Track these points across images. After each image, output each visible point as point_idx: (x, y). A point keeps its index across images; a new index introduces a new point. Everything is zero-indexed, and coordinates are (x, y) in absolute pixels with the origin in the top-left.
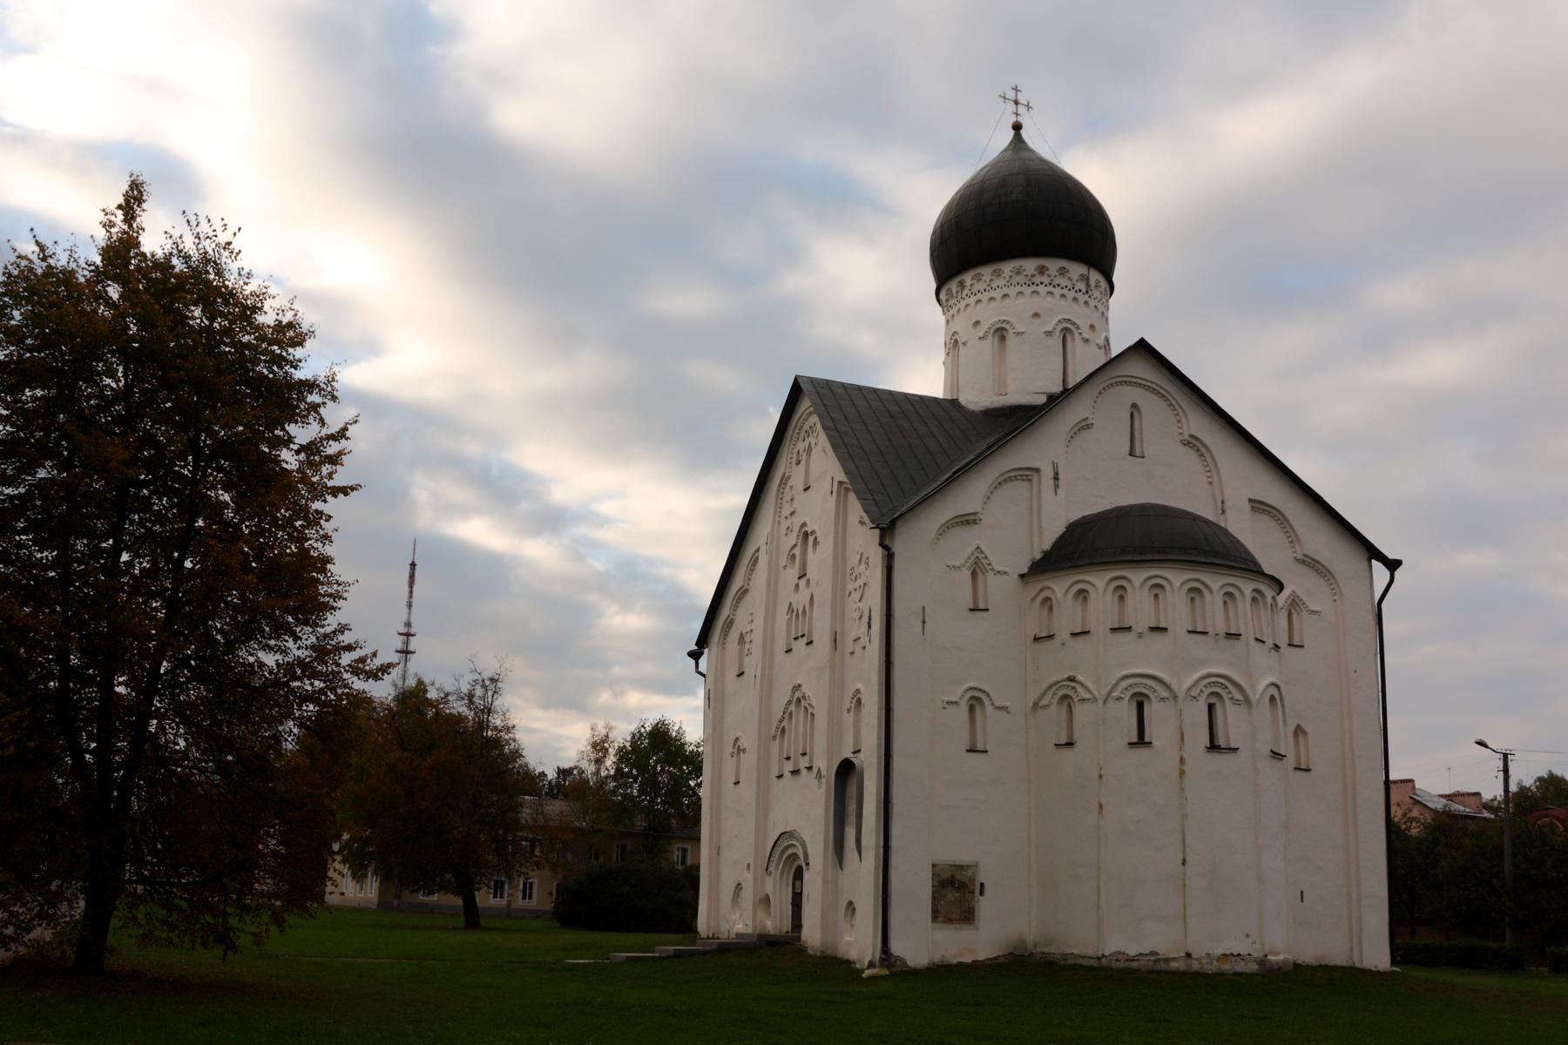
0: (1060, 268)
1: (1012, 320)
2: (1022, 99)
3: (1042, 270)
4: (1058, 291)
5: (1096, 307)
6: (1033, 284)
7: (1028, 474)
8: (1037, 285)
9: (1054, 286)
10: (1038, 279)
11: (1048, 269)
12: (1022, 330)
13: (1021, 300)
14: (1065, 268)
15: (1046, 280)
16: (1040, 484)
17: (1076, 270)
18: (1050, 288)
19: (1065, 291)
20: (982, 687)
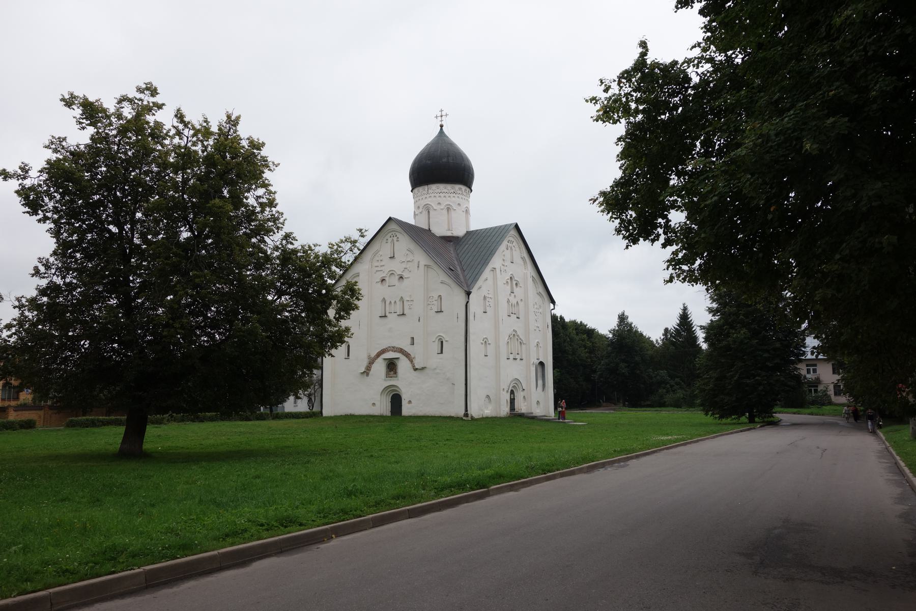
2: (439, 114)
3: (460, 189)
4: (463, 197)
10: (459, 192)
12: (455, 208)
15: (460, 192)
16: (496, 273)
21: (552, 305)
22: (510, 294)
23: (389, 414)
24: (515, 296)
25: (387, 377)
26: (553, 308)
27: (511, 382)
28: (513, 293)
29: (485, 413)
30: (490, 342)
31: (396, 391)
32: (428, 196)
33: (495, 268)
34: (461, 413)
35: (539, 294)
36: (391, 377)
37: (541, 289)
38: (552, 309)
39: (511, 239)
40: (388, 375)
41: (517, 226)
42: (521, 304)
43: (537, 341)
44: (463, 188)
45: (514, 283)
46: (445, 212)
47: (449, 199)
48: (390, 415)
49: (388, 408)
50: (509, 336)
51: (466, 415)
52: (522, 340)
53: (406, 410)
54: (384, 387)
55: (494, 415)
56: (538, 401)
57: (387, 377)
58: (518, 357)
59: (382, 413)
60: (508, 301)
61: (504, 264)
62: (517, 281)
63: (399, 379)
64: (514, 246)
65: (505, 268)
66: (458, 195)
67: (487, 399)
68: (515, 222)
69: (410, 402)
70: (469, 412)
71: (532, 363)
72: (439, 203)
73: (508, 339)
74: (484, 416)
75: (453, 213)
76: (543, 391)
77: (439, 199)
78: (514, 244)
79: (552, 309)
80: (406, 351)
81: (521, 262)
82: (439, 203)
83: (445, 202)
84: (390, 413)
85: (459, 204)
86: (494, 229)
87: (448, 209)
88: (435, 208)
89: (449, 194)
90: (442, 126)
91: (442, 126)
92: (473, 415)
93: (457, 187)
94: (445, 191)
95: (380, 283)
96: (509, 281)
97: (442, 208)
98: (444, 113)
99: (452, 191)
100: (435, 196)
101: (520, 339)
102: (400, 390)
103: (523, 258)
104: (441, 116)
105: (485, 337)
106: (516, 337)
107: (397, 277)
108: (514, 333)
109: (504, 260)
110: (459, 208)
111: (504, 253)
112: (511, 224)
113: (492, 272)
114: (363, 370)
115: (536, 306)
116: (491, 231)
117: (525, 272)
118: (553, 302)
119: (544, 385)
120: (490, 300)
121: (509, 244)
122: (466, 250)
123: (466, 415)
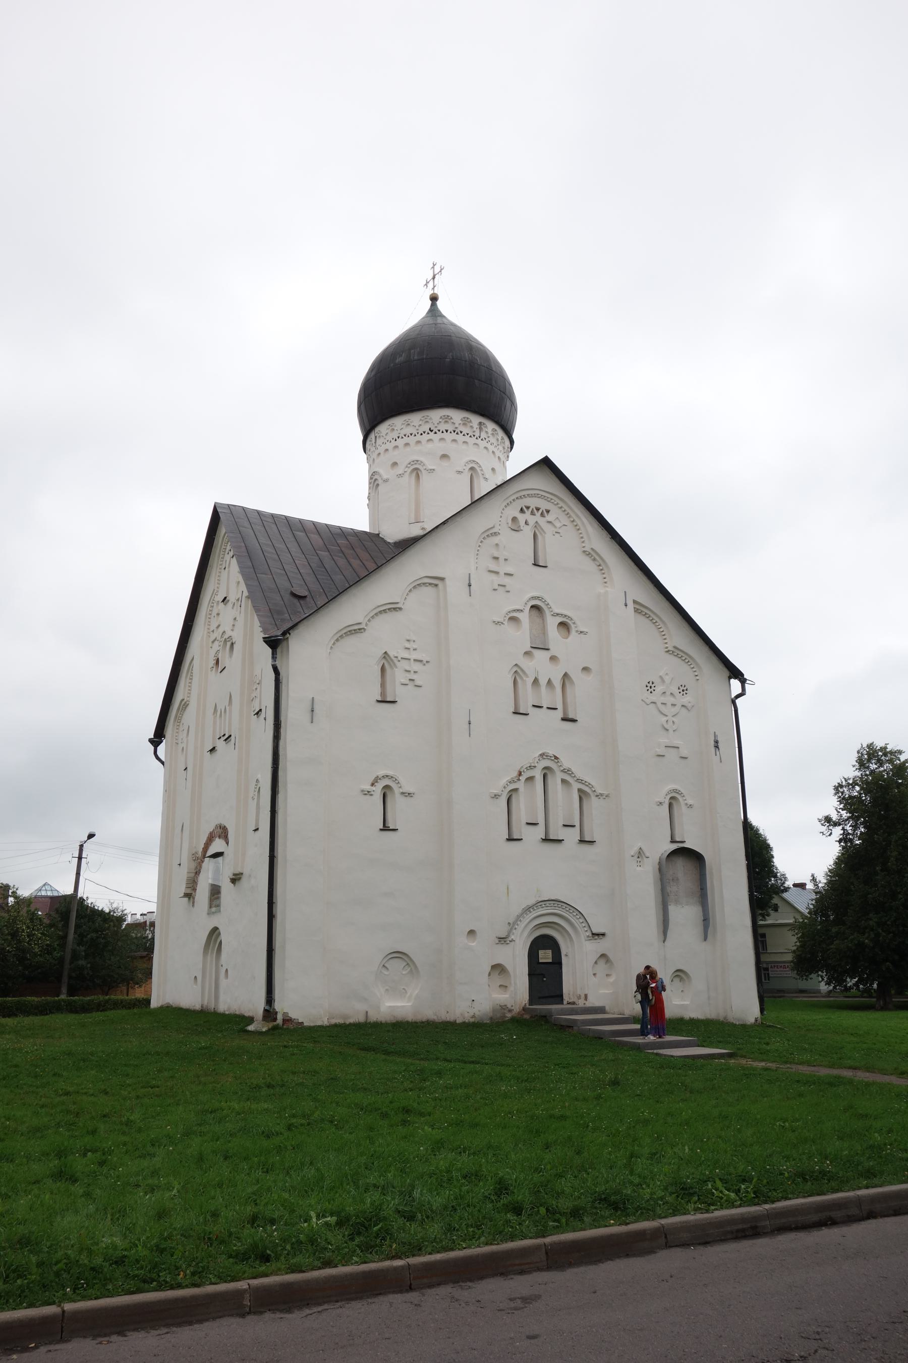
0: (464, 418)
1: (417, 458)
3: (447, 419)
4: (460, 438)
5: (493, 452)
6: (439, 431)
7: (436, 582)
8: (443, 432)
9: (457, 434)
10: (443, 427)
11: (451, 418)
13: (430, 445)
14: (468, 418)
17: (475, 420)
18: (454, 436)
19: (467, 438)
20: (390, 773)
21: (735, 685)
22: (527, 653)
24: (553, 658)
26: (740, 691)
27: (528, 909)
28: (548, 649)
29: (383, 1009)
30: (407, 788)
32: (377, 452)
33: (442, 579)
34: (254, 1005)
35: (676, 652)
37: (681, 638)
38: (738, 696)
39: (533, 503)
41: (546, 463)
42: (583, 686)
43: (673, 786)
44: (457, 416)
45: (552, 623)
46: (408, 481)
47: (419, 447)
50: (520, 774)
51: (269, 1014)
52: (589, 785)
54: (207, 933)
55: (430, 1012)
56: (678, 971)
58: (561, 833)
59: (206, 1003)
60: (517, 674)
61: (494, 567)
62: (566, 616)
63: (222, 909)
64: (549, 522)
65: (507, 580)
66: (445, 435)
67: (397, 965)
70: (278, 1006)
71: (635, 850)
72: (395, 464)
73: (512, 782)
74: (374, 1017)
75: (424, 476)
76: (705, 939)
77: (396, 452)
78: (549, 517)
79: (738, 696)
81: (589, 565)
82: (395, 464)
83: (405, 456)
85: (444, 456)
87: (417, 472)
88: (385, 477)
89: (418, 437)
90: (434, 299)
91: (434, 299)
92: (293, 1015)
93: (436, 415)
94: (408, 430)
95: (215, 666)
96: (524, 617)
97: (401, 472)
98: (437, 269)
99: (426, 428)
100: (387, 450)
101: (579, 781)
103: (591, 554)
104: (434, 278)
105: (381, 773)
106: (559, 776)
107: (229, 644)
108: (547, 763)
109: (496, 558)
110: (445, 463)
111: (496, 540)
113: (430, 590)
114: (182, 889)
115: (659, 689)
117: (602, 591)
118: (735, 673)
119: (706, 921)
120: (416, 667)
121: (522, 518)
123: (269, 1014)
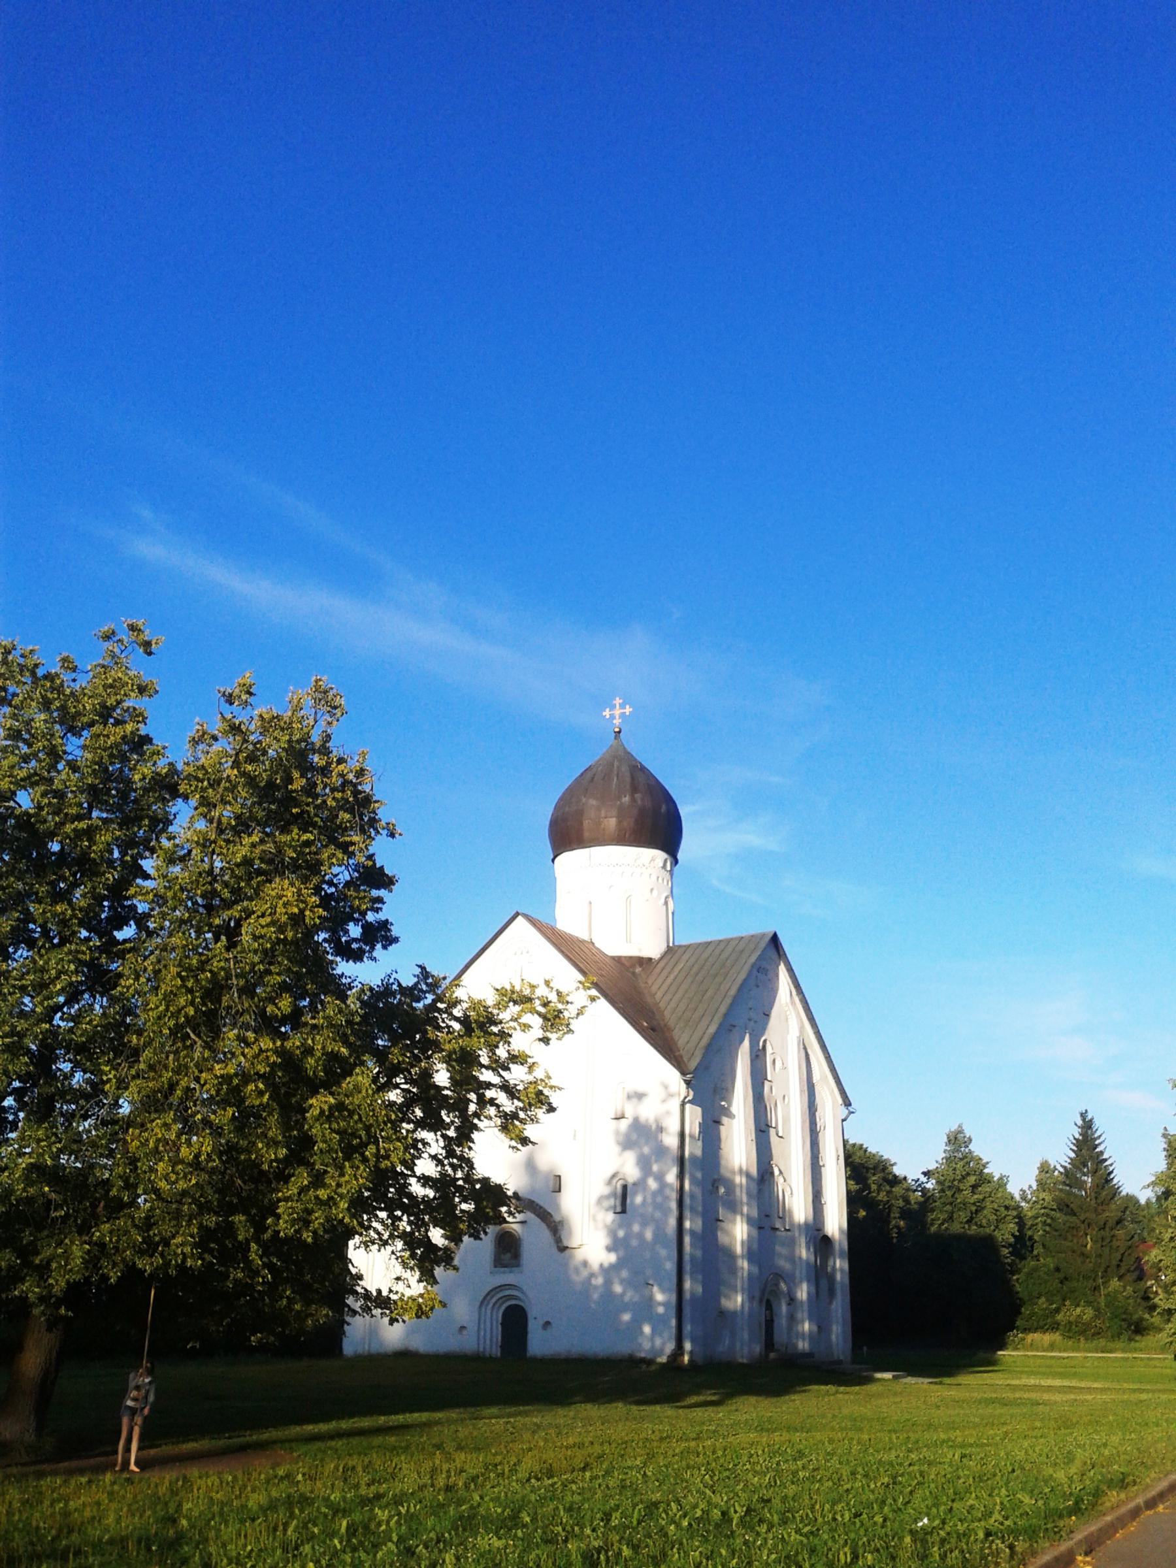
23: (496, 1352)
25: (495, 1267)
31: (516, 1298)
36: (506, 1266)
40: (498, 1262)
48: (499, 1354)
49: (495, 1340)
53: (539, 1343)
57: (495, 1267)
68: (768, 929)
69: (547, 1324)
80: (541, 1207)
84: (499, 1349)
86: (761, 939)
102: (523, 1293)
112: (764, 935)
116: (722, 946)
122: (671, 984)
